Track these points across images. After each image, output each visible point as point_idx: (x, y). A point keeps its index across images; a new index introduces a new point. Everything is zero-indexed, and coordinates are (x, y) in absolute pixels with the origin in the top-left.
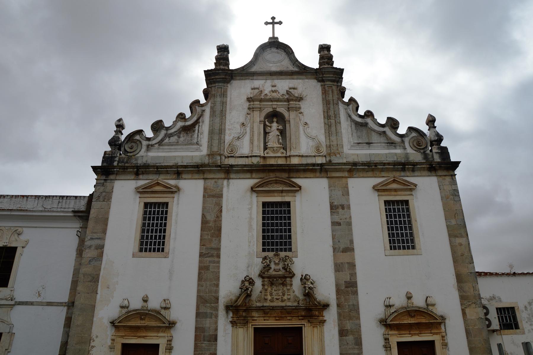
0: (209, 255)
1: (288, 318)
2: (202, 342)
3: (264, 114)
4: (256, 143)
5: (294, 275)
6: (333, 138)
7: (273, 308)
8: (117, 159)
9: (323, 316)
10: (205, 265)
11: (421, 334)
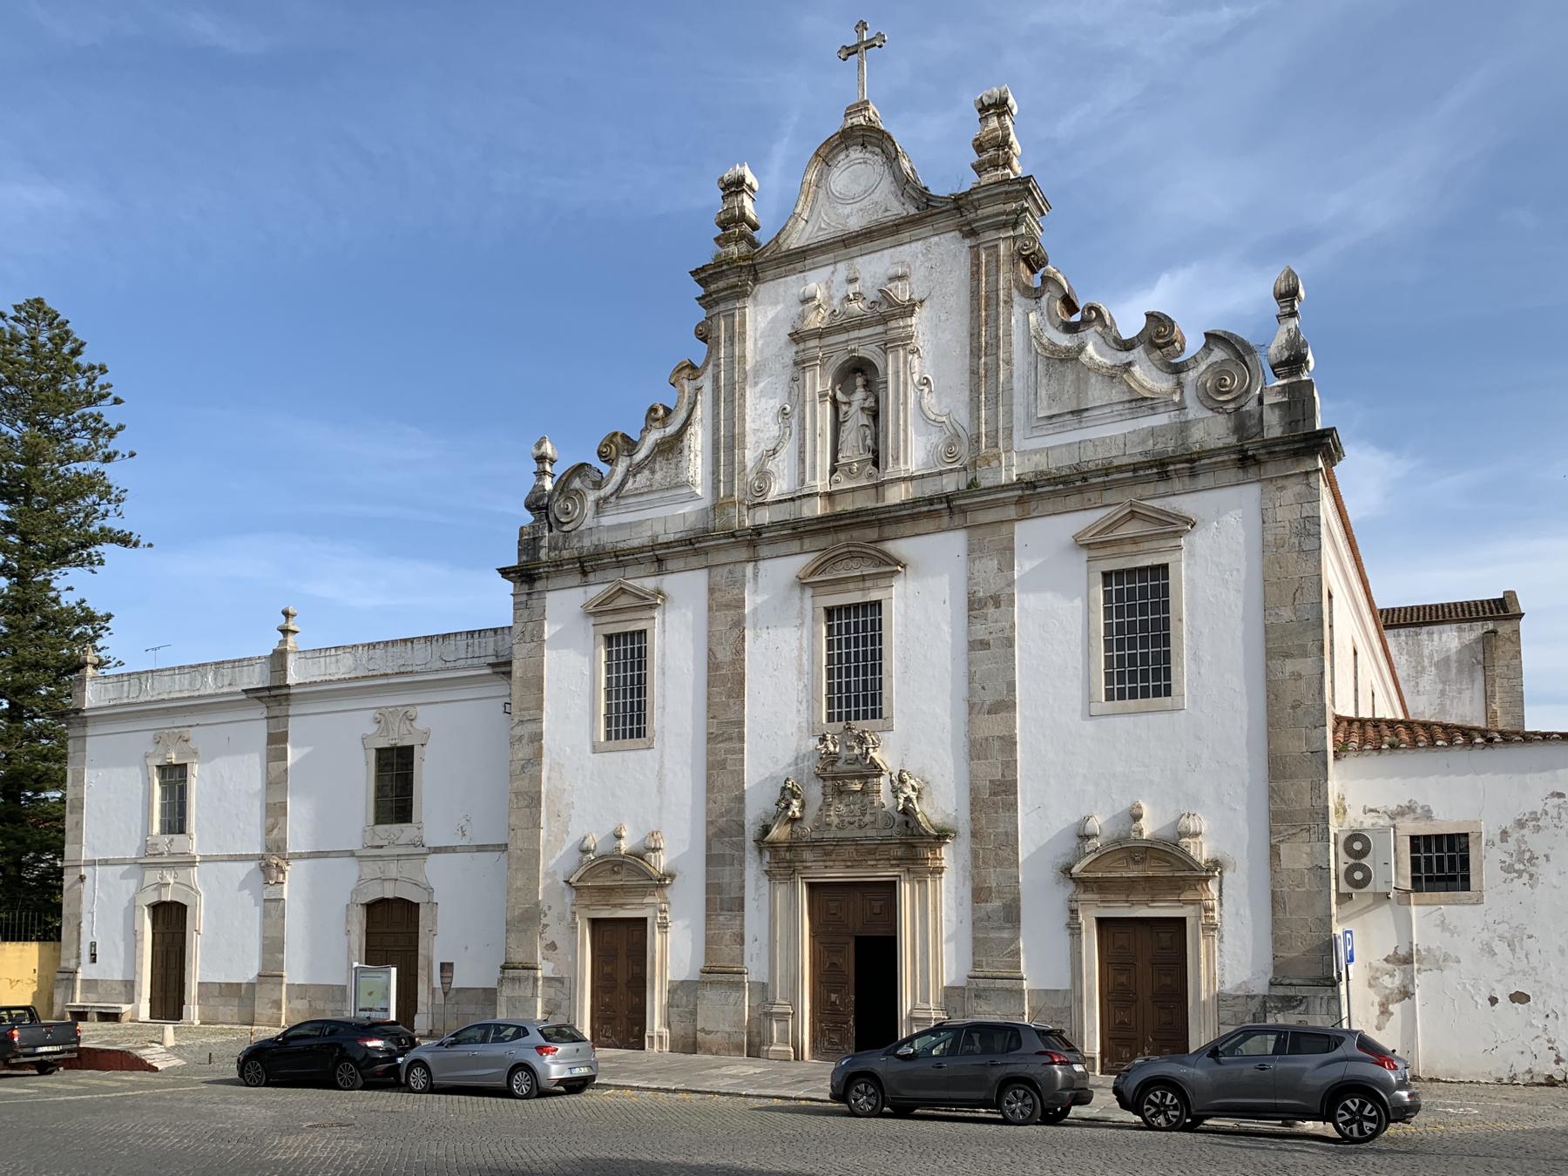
7: (839, 842)
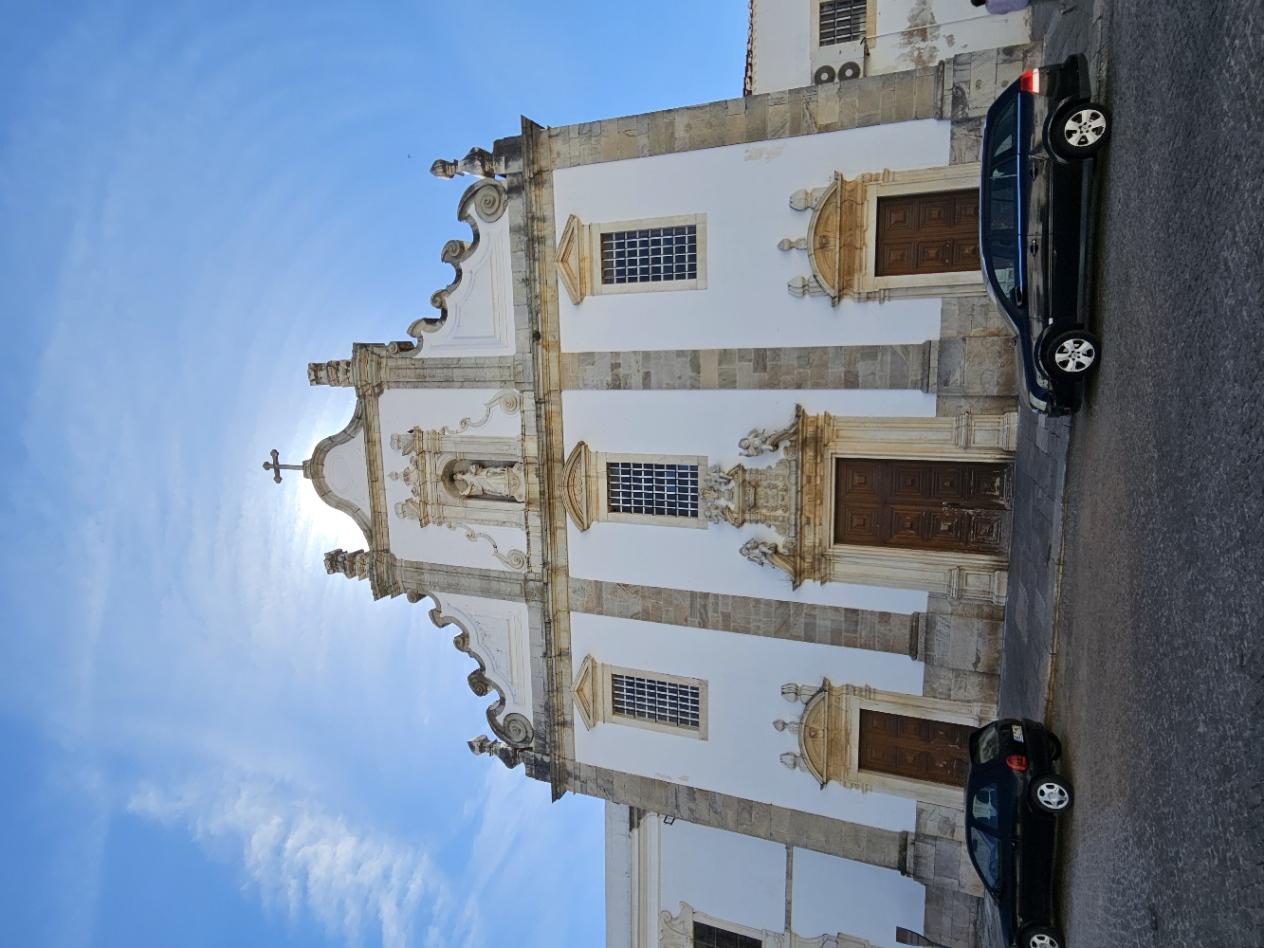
0: (702, 611)
1: (818, 482)
2: (858, 635)
3: (450, 499)
4: (501, 516)
5: (739, 466)
6: (489, 374)
7: (800, 509)
8: (539, 756)
9: (817, 418)
10: (720, 619)
11: (862, 226)
